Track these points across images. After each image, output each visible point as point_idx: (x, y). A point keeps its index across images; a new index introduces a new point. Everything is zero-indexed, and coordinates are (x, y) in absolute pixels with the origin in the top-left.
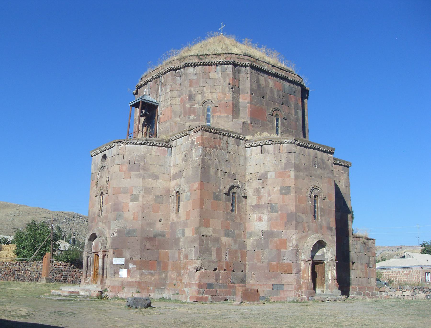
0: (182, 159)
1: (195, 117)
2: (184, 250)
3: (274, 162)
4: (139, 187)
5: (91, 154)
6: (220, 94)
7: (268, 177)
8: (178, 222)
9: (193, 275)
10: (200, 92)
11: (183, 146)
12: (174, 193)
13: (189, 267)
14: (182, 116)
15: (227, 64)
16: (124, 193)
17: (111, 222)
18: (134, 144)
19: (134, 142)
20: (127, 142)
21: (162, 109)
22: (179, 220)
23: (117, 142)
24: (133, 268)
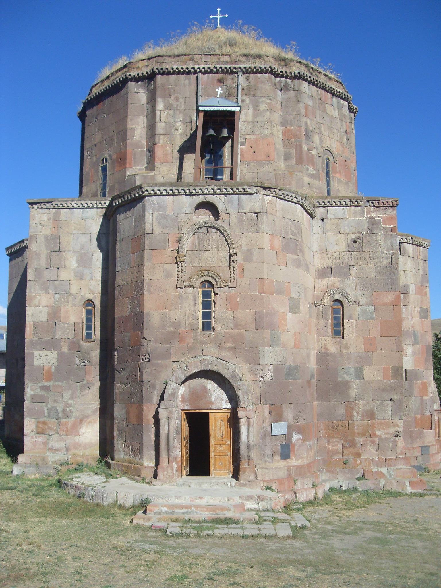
0: (344, 244)
1: (314, 172)
2: (361, 402)
3: (414, 270)
4: (298, 285)
5: (149, 189)
6: (338, 144)
7: (409, 292)
8: (341, 355)
9: (391, 445)
10: (317, 131)
11: (346, 223)
12: (327, 301)
13: (378, 433)
14: (294, 162)
15: (344, 99)
16: (279, 292)
17: (261, 349)
18: (290, 199)
19: (291, 196)
20: (281, 193)
21: (248, 137)
22: (344, 350)
23: (262, 187)
24: (298, 440)
